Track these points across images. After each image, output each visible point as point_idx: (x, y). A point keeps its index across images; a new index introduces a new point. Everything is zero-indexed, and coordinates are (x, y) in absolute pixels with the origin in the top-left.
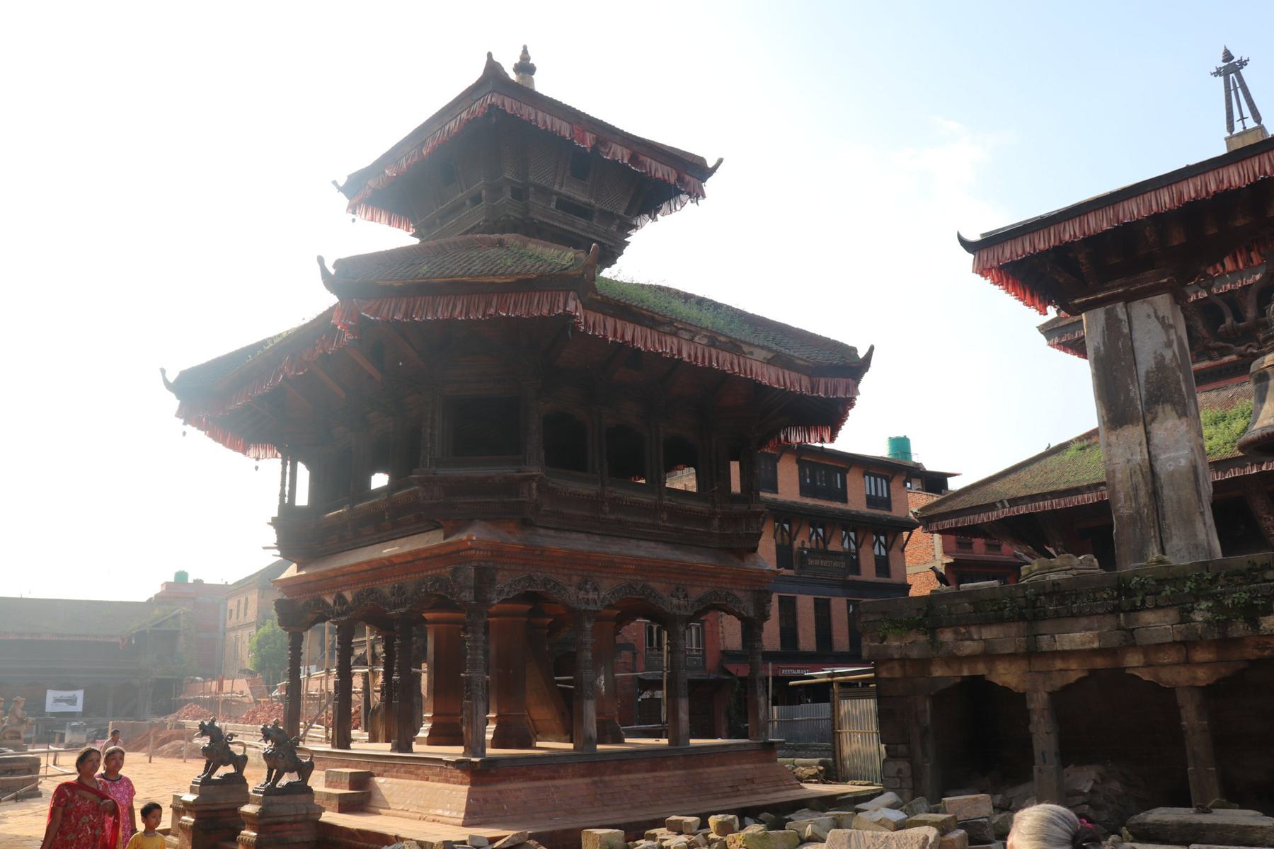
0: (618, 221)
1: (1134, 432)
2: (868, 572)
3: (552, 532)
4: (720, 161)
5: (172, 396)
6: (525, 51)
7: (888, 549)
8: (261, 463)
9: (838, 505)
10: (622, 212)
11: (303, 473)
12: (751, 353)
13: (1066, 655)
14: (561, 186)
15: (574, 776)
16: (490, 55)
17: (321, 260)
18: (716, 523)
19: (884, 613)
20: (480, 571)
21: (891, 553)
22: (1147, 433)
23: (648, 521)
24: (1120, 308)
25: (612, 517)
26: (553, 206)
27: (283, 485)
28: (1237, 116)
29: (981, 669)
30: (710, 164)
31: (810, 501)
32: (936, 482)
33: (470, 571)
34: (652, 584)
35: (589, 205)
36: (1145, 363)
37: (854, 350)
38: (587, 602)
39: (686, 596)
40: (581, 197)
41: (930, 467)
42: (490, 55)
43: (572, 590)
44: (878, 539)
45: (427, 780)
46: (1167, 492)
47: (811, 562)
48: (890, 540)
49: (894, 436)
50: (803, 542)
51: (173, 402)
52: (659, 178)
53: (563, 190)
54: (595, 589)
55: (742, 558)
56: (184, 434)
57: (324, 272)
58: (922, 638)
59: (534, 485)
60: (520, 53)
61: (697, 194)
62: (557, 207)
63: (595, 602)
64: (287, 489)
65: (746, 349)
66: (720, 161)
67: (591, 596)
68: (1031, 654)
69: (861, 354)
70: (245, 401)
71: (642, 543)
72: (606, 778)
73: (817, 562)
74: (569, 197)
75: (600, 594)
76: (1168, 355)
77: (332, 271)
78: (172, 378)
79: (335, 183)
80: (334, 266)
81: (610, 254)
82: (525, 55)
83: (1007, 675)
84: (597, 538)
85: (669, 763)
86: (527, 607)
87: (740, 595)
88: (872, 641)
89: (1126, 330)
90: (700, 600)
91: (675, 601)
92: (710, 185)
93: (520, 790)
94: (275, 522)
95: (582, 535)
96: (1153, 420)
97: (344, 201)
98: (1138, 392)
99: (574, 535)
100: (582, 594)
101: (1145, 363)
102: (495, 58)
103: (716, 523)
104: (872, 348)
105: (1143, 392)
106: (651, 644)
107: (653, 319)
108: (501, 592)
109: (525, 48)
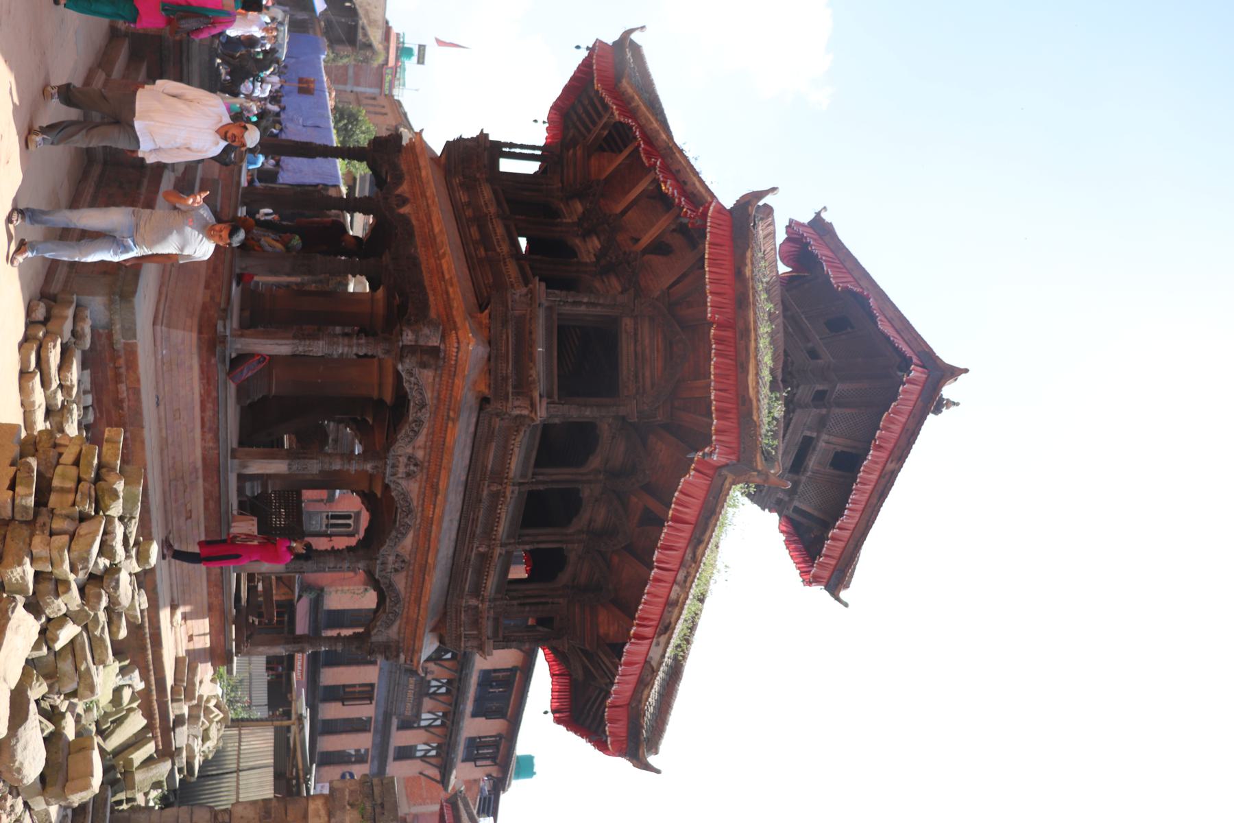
2: (399, 738)
3: (472, 429)
4: (846, 605)
5: (616, 37)
7: (424, 758)
9: (469, 707)
10: (796, 503)
11: (531, 167)
14: (827, 442)
15: (204, 449)
16: (966, 371)
18: (473, 602)
19: (382, 805)
20: (435, 351)
21: (419, 762)
23: (478, 531)
25: (485, 493)
26: (808, 433)
27: (522, 146)
31: (474, 680)
33: (435, 342)
34: (410, 535)
35: (805, 470)
38: (393, 466)
39: (396, 570)
40: (812, 462)
41: (504, 798)
42: (966, 371)
43: (409, 450)
44: (433, 748)
45: (207, 287)
47: (412, 680)
48: (433, 761)
49: (535, 761)
50: (432, 672)
51: (610, 38)
53: (822, 444)
55: (433, 630)
56: (578, 47)
57: (760, 195)
59: (525, 412)
61: (810, 579)
62: (805, 437)
63: (394, 474)
64: (518, 150)
65: (663, 639)
66: (846, 605)
67: (402, 470)
69: (652, 759)
70: (608, 113)
71: (456, 524)
72: (200, 481)
73: (411, 686)
74: (814, 449)
77: (761, 203)
78: (634, 37)
80: (765, 205)
84: (463, 478)
86: (388, 397)
87: (395, 628)
88: (351, 792)
90: (391, 585)
91: (391, 559)
92: (819, 593)
93: (192, 389)
94: (483, 136)
95: (467, 461)
99: (468, 453)
100: (403, 460)
102: (962, 377)
103: (473, 602)
104: (658, 772)
106: (334, 517)
107: (700, 542)
108: (411, 374)
109: (957, 404)
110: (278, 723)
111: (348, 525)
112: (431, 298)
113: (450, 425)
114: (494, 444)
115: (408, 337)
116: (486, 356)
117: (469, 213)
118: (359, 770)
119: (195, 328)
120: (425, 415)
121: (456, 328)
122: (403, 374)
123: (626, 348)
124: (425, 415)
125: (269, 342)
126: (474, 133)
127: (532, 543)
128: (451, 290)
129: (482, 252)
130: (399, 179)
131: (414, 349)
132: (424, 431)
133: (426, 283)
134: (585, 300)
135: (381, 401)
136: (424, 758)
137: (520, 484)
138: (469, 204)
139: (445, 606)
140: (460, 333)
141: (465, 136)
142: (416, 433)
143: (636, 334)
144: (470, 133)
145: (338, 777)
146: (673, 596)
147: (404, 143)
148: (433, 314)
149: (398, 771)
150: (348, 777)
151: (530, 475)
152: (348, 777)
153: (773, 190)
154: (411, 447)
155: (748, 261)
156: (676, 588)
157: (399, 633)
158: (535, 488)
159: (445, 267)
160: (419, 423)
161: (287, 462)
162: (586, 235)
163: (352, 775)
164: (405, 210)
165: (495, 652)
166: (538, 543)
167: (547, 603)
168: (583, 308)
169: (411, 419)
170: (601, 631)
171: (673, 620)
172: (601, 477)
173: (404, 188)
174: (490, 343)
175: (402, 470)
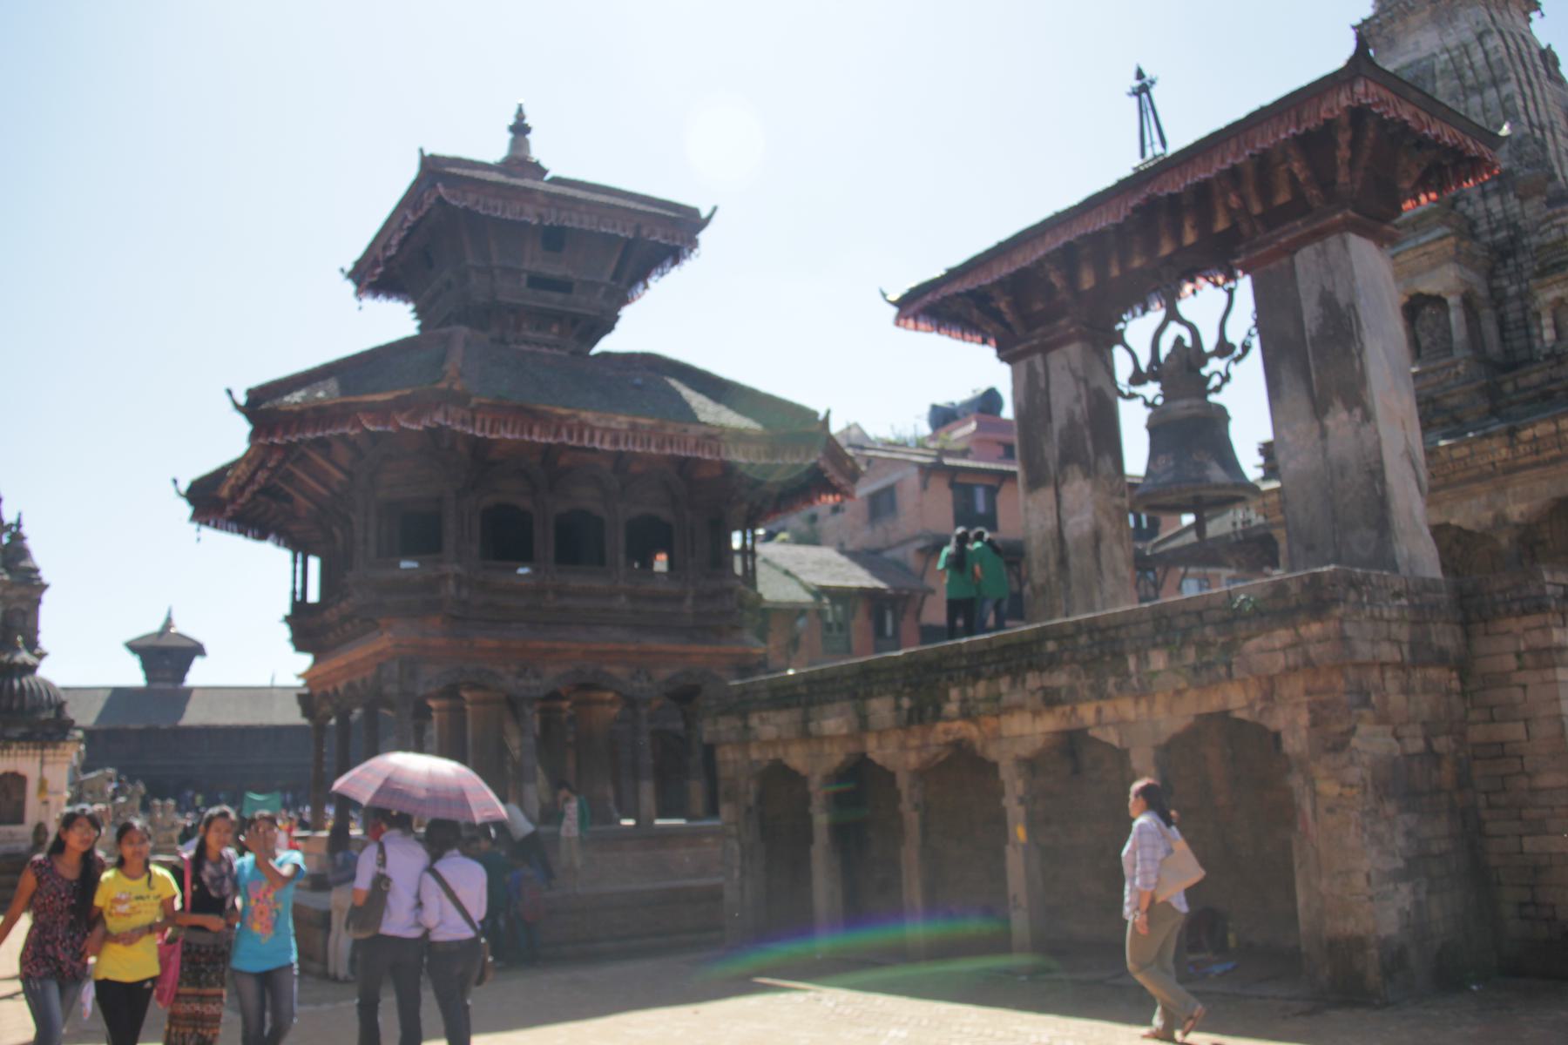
0: (603, 289)
1: (1047, 494)
4: (715, 209)
6: (520, 110)
10: (607, 278)
13: (832, 738)
17: (230, 392)
18: (689, 602)
22: (1058, 496)
24: (1038, 359)
26: (524, 284)
28: (1147, 141)
29: (780, 752)
30: (704, 214)
34: (607, 668)
36: (1059, 422)
37: (815, 414)
39: (650, 679)
46: (1073, 560)
51: (187, 509)
52: (655, 236)
58: (739, 724)
60: (514, 111)
64: (299, 587)
66: (715, 209)
68: (805, 735)
69: (821, 416)
76: (1078, 410)
78: (184, 486)
79: (342, 270)
81: (606, 324)
82: (520, 115)
83: (796, 758)
89: (1042, 384)
94: (288, 619)
96: (1064, 481)
97: (350, 287)
98: (1052, 451)
100: (522, 682)
101: (1059, 422)
103: (689, 602)
105: (1057, 452)
144: (285, 632)
153: (230, 392)
173: (330, 689)
175: (533, 682)
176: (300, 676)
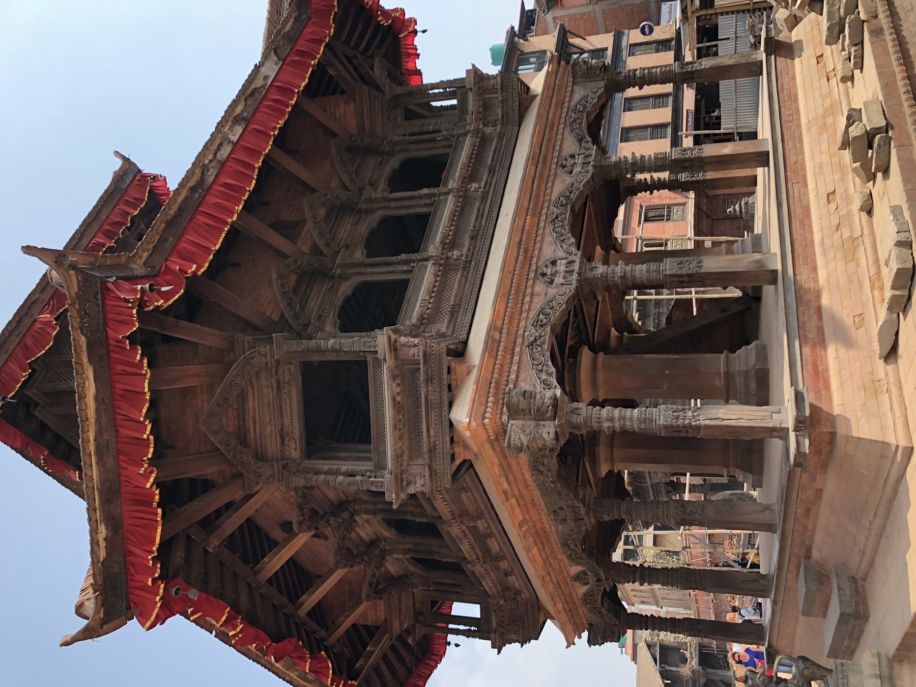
8: (453, 643)
12: (266, 78)
18: (488, 130)
32: (528, 19)
43: (552, 291)
45: (819, 492)
48: (575, 50)
49: (491, 61)
54: (554, 263)
64: (462, 627)
65: (258, 83)
67: (561, 267)
75: (558, 249)
85: (792, 159)
86: (586, 354)
87: (577, 97)
100: (559, 280)
103: (488, 130)
108: (547, 385)
110: (710, 11)
111: (646, 246)
112: (528, 476)
113: (499, 323)
114: (452, 302)
115: (548, 431)
116: (454, 408)
117: (504, 565)
118: (635, 36)
119: (840, 441)
120: (532, 333)
121: (490, 442)
122: (555, 383)
123: (294, 422)
124: (532, 333)
125: (733, 423)
126: (507, 648)
127: (420, 197)
128: (506, 485)
129: (481, 525)
130: (587, 598)
131: (539, 416)
132: (533, 314)
133: (537, 493)
134: (340, 478)
135: (593, 349)
136: (582, 51)
137: (427, 260)
138: (506, 574)
139: (520, 126)
140: (484, 437)
141: (518, 645)
142: (541, 311)
143: (282, 439)
144: (512, 649)
145: (656, 28)
146: (239, 130)
147: (585, 635)
148: (524, 458)
149: (604, 41)
150: (647, 30)
151: (416, 271)
152: (647, 30)
154: (553, 295)
155: (103, 544)
156: (234, 138)
157: (572, 92)
158: (413, 256)
159: (518, 511)
160: (538, 324)
161: (703, 270)
162: (373, 543)
163: (643, 33)
164: (575, 569)
165: (464, 75)
166: (411, 198)
167: (410, 135)
168: (344, 468)
169: (548, 329)
170: (352, 106)
171: (243, 103)
172: (338, 271)
173: (582, 590)
174: (451, 424)
175: (561, 267)
176: (570, 643)
